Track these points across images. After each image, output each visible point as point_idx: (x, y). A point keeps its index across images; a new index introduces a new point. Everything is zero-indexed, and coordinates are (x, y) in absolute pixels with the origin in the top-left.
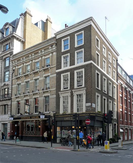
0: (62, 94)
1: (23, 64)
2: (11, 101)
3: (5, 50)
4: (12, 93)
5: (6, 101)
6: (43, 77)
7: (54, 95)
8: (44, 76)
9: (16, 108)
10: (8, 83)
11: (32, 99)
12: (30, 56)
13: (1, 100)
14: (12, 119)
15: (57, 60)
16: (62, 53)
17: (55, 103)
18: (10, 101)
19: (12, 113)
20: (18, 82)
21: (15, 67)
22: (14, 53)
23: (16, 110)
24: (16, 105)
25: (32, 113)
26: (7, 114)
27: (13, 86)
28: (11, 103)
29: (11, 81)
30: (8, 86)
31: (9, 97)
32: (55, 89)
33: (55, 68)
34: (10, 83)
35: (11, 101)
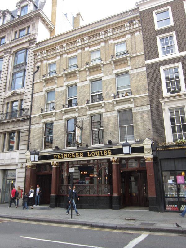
0: (166, 104)
1: (61, 56)
2: (30, 123)
3: (17, 36)
4: (34, 109)
5: (15, 125)
6: (112, 74)
7: (145, 107)
8: (115, 72)
9: (42, 137)
10: (22, 91)
11: (87, 117)
13: (5, 121)
14: (37, 157)
15: (144, 44)
17: (150, 122)
18: (28, 123)
19: (32, 147)
20: (46, 87)
21: (41, 62)
22: (38, 41)
23: (42, 140)
24: (43, 130)
25: (87, 146)
26: (18, 148)
27: (34, 95)
28: (30, 128)
29: (31, 86)
30: (22, 95)
31: (27, 116)
32: (148, 94)
33: (143, 57)
34: (27, 90)
35: (30, 123)
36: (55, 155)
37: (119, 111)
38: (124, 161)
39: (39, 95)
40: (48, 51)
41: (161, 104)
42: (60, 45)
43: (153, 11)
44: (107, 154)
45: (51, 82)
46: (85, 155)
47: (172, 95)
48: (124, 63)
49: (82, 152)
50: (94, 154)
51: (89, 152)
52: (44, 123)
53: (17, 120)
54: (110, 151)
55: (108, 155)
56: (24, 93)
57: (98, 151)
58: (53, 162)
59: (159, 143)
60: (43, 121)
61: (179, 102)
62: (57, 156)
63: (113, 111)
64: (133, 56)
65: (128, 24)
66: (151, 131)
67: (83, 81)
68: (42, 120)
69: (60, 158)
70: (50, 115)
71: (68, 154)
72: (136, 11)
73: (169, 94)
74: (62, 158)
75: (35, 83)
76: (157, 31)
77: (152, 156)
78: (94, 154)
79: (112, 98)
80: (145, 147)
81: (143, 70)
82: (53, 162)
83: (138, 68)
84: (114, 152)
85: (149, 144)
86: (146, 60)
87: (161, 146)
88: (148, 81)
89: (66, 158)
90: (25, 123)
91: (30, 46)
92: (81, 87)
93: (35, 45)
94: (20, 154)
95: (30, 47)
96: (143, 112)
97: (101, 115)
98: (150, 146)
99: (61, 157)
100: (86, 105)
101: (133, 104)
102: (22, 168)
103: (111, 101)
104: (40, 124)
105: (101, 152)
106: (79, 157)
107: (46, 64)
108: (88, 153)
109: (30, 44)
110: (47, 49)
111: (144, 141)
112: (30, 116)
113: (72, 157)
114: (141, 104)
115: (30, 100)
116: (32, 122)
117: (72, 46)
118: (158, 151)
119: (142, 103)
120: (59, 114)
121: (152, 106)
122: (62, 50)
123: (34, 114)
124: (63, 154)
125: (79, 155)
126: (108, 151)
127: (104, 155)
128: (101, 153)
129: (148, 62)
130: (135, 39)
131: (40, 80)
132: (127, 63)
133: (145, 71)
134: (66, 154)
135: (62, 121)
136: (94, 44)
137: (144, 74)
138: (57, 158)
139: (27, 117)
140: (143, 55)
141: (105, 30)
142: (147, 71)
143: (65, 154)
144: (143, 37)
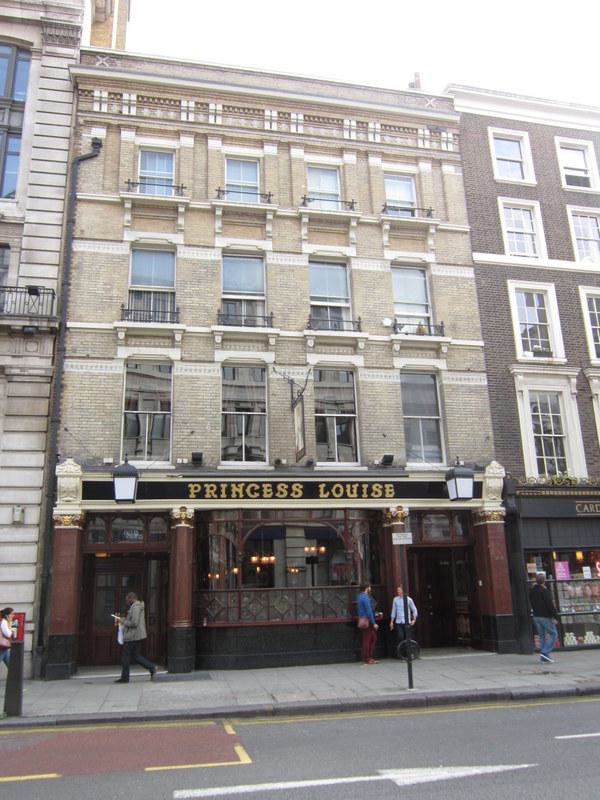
6: (381, 258)
11: (305, 370)
12: (271, 113)
15: (467, 204)
17: (488, 419)
27: (77, 246)
32: (482, 343)
36: (194, 483)
37: (404, 371)
38: (99, 521)
39: (101, 251)
40: (142, 101)
41: (512, 377)
42: (197, 99)
44: (380, 494)
45: (155, 218)
46: (311, 491)
47: (537, 359)
48: (413, 238)
49: (301, 483)
50: (342, 490)
51: (324, 485)
52: (127, 362)
54: (392, 486)
55: (262, 498)
57: (355, 483)
58: (183, 509)
60: (124, 352)
61: (551, 381)
62: (204, 489)
63: (390, 368)
65: (427, 132)
66: (492, 441)
67: (289, 253)
68: (120, 349)
69: (212, 498)
71: (247, 484)
73: (529, 356)
74: (224, 495)
75: (80, 200)
77: (503, 509)
78: (342, 490)
79: (385, 331)
81: (467, 276)
82: (183, 509)
83: (454, 265)
84: (405, 490)
89: (238, 497)
90: (32, 347)
92: (282, 269)
93: (75, 53)
96: (471, 390)
97: (167, 366)
98: (499, 483)
99: (218, 492)
100: (307, 332)
103: (386, 338)
104: (113, 363)
105: (365, 486)
106: (289, 497)
107: (133, 143)
108: (322, 486)
109: (47, 39)
110: (143, 93)
111: (487, 469)
112: (63, 325)
113: (261, 497)
114: (464, 367)
115: (55, 258)
116: (68, 346)
117: (243, 122)
119: (468, 365)
120: (194, 340)
122: (201, 118)
123: (81, 316)
124: (229, 484)
125: (287, 490)
126: (387, 486)
127: (372, 498)
128: (365, 491)
129: (480, 257)
131: (114, 197)
132: (424, 240)
134: (241, 483)
135: (209, 366)
136: (322, 148)
138: (201, 495)
139: (52, 325)
140: (466, 233)
141: (362, 119)
143: (237, 483)
144: (465, 187)
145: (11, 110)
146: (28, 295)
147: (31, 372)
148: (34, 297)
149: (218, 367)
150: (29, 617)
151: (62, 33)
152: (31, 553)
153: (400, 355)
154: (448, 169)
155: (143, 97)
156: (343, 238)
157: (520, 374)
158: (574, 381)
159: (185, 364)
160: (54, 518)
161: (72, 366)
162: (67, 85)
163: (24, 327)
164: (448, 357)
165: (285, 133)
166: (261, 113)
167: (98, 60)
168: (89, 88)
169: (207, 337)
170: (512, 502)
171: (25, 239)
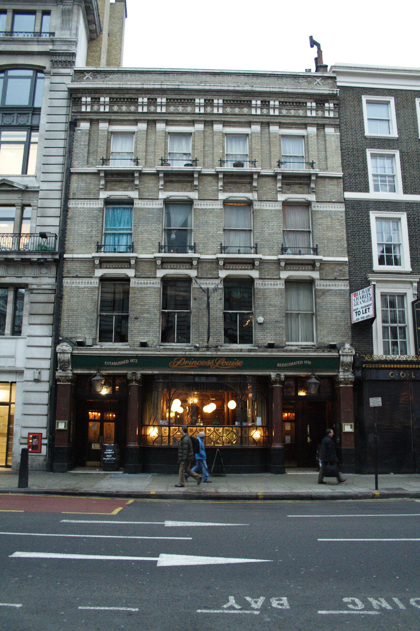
7: (341, 283)
10: (30, 185)
11: (217, 281)
15: (342, 156)
16: (365, 138)
26: (17, 331)
27: (72, 204)
30: (27, 195)
32: (346, 259)
42: (149, 96)
43: (363, 97)
45: (121, 181)
53: (23, 260)
56: (38, 191)
58: (134, 374)
59: (366, 355)
61: (399, 285)
63: (277, 279)
64: (322, 174)
65: (314, 104)
68: (96, 271)
70: (125, 262)
72: (330, 81)
75: (72, 173)
76: (367, 139)
80: (343, 359)
81: (339, 209)
85: (351, 356)
86: (345, 190)
87: (369, 360)
88: (347, 233)
90: (44, 271)
91: (53, 67)
92: (204, 211)
94: (28, 346)
95: (55, 71)
101: (318, 272)
102: (37, 381)
104: (92, 280)
109: (54, 64)
112: (61, 256)
115: (57, 212)
117: (180, 109)
118: (364, 368)
121: (353, 284)
123: (73, 250)
129: (349, 195)
130: (325, 140)
132: (308, 185)
133: (341, 212)
137: (341, 217)
140: (340, 178)
142: (346, 212)
145: (33, 114)
146: (40, 238)
147: (43, 287)
148: (44, 239)
149: (159, 281)
150: (44, 436)
151: (63, 59)
152: (45, 398)
153: (285, 269)
154: (329, 131)
155: (113, 99)
156: (248, 186)
157: (374, 281)
158: (415, 285)
159: (137, 279)
160: (57, 377)
161: (67, 283)
162: (65, 95)
163: (38, 259)
164: (320, 269)
165: (210, 114)
166: (193, 101)
167: (85, 76)
168: (79, 95)
169: (151, 261)
170: (359, 373)
171: (40, 201)
